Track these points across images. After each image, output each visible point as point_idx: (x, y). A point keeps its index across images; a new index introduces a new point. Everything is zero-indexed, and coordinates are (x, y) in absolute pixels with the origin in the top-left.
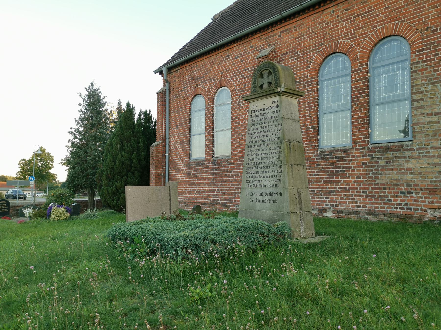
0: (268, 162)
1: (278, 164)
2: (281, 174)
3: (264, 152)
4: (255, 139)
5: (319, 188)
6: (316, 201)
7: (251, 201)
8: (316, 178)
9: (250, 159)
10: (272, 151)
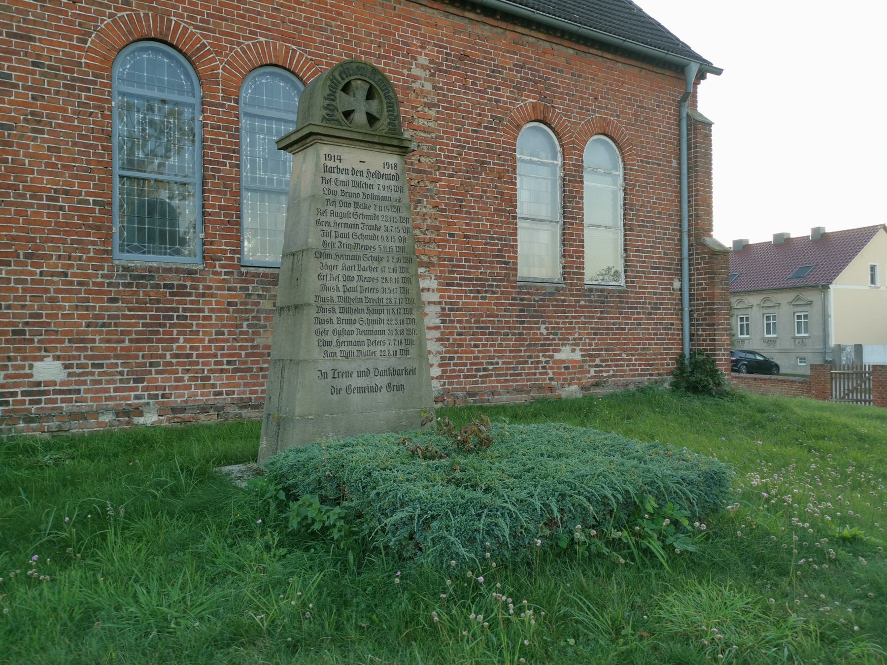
0: (380, 300)
1: (404, 305)
2: (411, 327)
3: (367, 274)
4: (339, 239)
5: (117, 357)
6: (107, 390)
7: (336, 391)
8: (108, 333)
9: (325, 288)
10: (387, 275)
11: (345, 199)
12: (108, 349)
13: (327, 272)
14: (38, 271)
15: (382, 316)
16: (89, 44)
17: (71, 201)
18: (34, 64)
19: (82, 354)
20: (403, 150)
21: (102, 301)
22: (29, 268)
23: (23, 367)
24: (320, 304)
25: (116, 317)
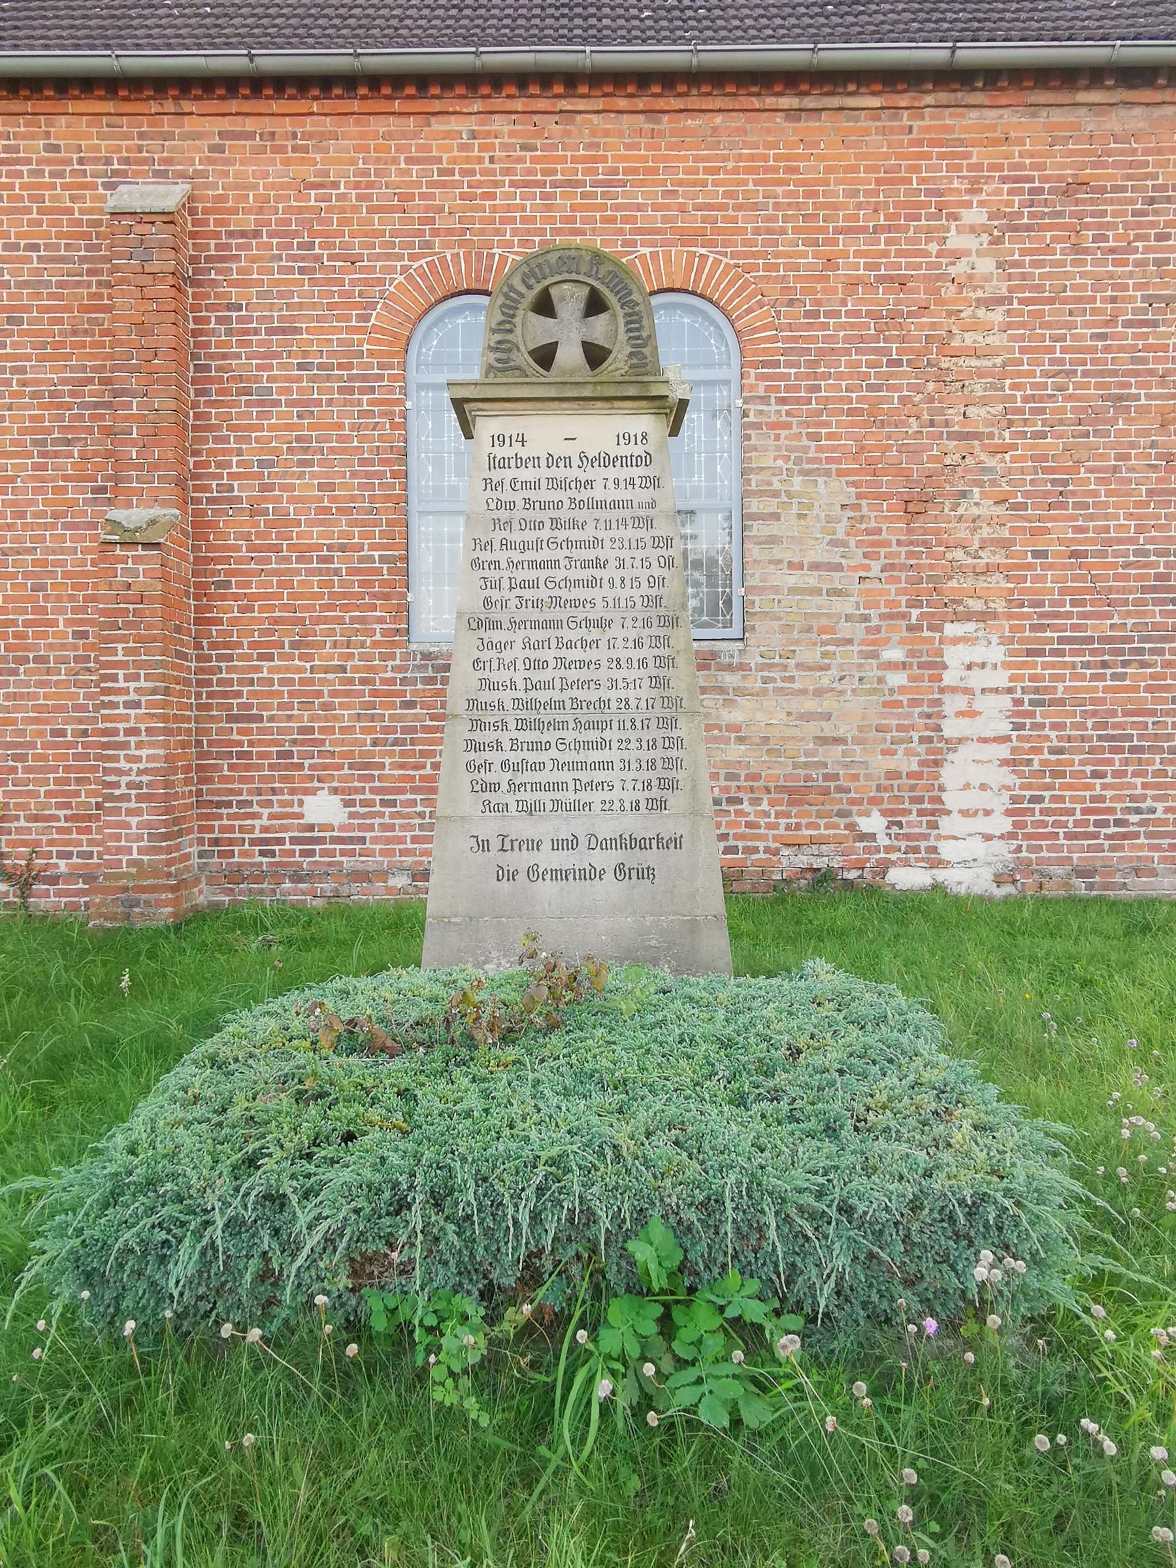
0: (603, 703)
1: (658, 711)
2: (673, 753)
3: (577, 654)
4: (518, 592)
5: (415, 790)
6: (401, 840)
7: (505, 874)
8: (403, 754)
9: (487, 684)
10: (623, 655)
11: (531, 515)
12: (403, 779)
13: (493, 654)
14: (308, 665)
15: (607, 735)
16: (373, 321)
17: (349, 560)
18: (301, 367)
19: (367, 786)
20: (657, 403)
21: (392, 706)
22: (297, 662)
23: (290, 804)
24: (476, 714)
25: (413, 730)
